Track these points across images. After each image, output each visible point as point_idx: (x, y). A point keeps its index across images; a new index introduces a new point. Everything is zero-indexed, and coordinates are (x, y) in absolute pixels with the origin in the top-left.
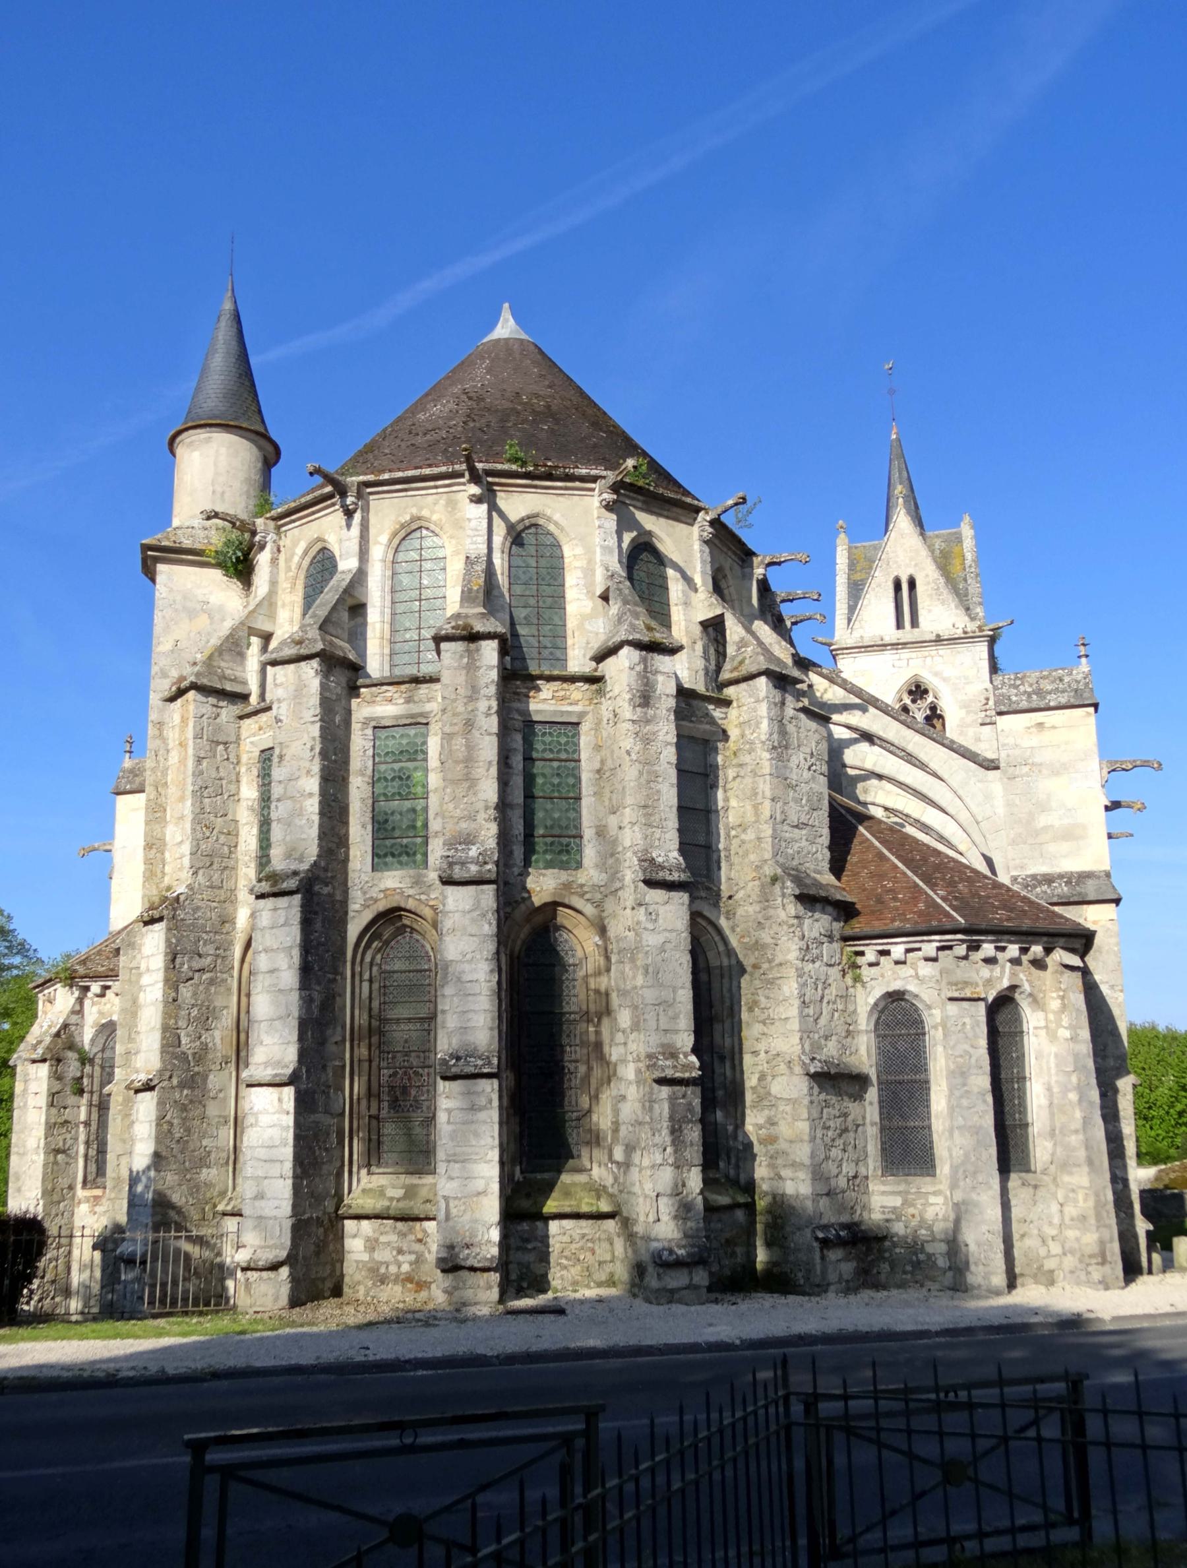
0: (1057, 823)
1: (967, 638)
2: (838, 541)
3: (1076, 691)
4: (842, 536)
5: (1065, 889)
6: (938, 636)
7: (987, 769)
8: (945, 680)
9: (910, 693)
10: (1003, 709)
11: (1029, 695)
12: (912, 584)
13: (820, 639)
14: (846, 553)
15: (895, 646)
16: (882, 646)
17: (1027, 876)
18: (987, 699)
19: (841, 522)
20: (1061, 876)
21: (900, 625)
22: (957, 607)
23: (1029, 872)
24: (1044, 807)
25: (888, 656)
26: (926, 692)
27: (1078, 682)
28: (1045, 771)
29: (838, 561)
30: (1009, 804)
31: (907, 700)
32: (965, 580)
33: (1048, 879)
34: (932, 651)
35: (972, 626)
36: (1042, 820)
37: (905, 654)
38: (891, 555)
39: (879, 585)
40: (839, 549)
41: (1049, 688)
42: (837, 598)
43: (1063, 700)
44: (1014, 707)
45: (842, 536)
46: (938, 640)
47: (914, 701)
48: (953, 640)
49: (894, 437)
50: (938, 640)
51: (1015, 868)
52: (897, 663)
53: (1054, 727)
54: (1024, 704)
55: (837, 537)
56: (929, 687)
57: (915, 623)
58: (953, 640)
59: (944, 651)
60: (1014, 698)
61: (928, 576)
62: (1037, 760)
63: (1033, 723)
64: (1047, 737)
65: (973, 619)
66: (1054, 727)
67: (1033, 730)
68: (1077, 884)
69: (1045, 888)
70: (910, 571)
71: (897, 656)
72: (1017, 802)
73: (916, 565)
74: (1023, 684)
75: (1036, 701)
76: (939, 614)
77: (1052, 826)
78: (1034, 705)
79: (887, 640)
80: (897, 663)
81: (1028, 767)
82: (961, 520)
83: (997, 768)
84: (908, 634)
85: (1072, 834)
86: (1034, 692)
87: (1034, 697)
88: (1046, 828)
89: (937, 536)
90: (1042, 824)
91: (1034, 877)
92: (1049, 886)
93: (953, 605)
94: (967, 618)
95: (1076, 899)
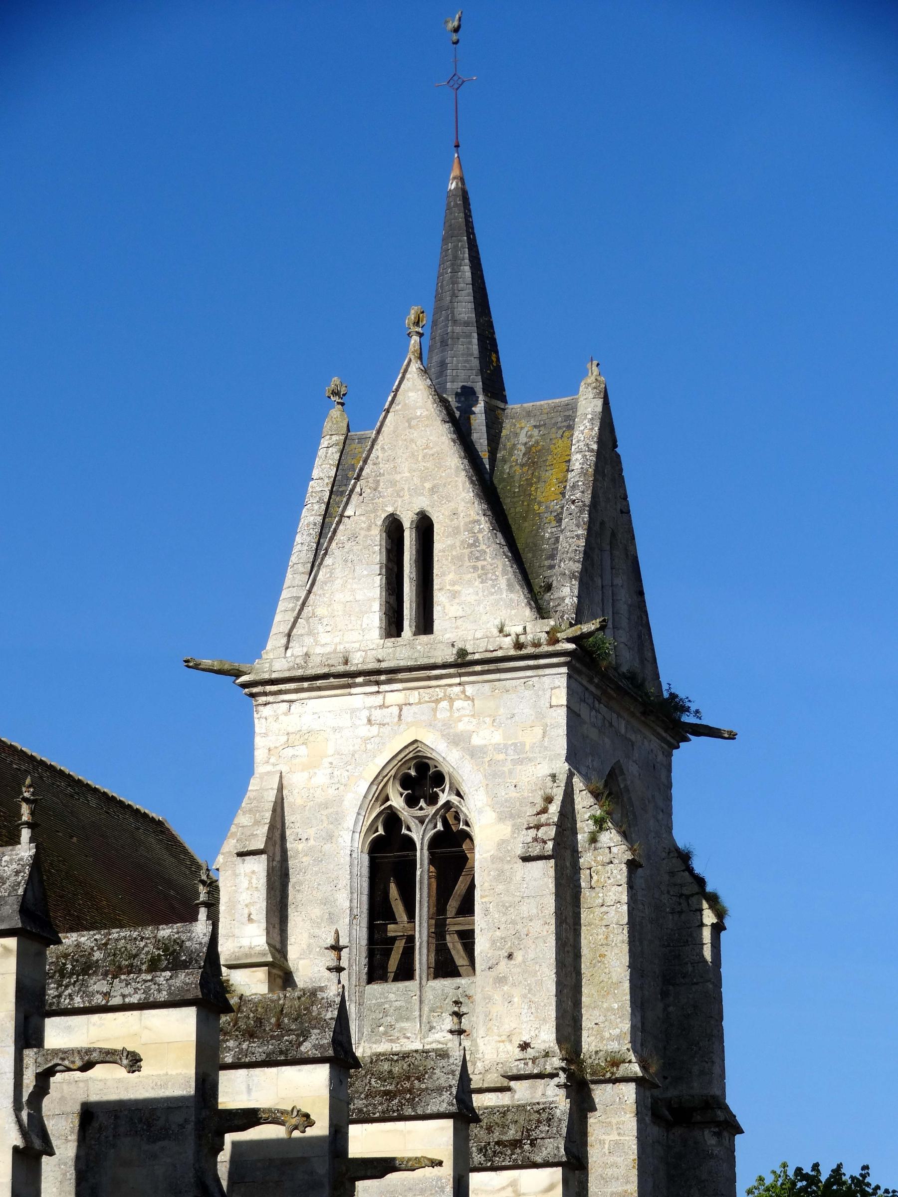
1: (522, 657)
2: (327, 425)
4: (335, 412)
6: (462, 653)
8: (474, 753)
9: (406, 782)
12: (425, 527)
13: (207, 662)
14: (334, 454)
15: (378, 675)
16: (343, 678)
18: (549, 800)
19: (336, 380)
21: (393, 625)
22: (510, 586)
25: (360, 699)
26: (439, 779)
29: (315, 473)
31: (397, 802)
32: (559, 520)
34: (451, 686)
35: (537, 630)
37: (395, 694)
38: (384, 467)
39: (354, 537)
40: (325, 442)
42: (294, 559)
46: (463, 663)
47: (411, 802)
48: (493, 664)
49: (452, 186)
50: (463, 663)
52: (377, 714)
55: (325, 415)
56: (445, 769)
57: (425, 625)
58: (493, 664)
59: (476, 688)
61: (458, 512)
65: (542, 612)
70: (422, 503)
71: (378, 700)
73: (433, 490)
76: (478, 602)
79: (358, 662)
80: (377, 714)
82: (584, 374)
84: (410, 648)
89: (529, 414)
93: (503, 582)
94: (528, 613)
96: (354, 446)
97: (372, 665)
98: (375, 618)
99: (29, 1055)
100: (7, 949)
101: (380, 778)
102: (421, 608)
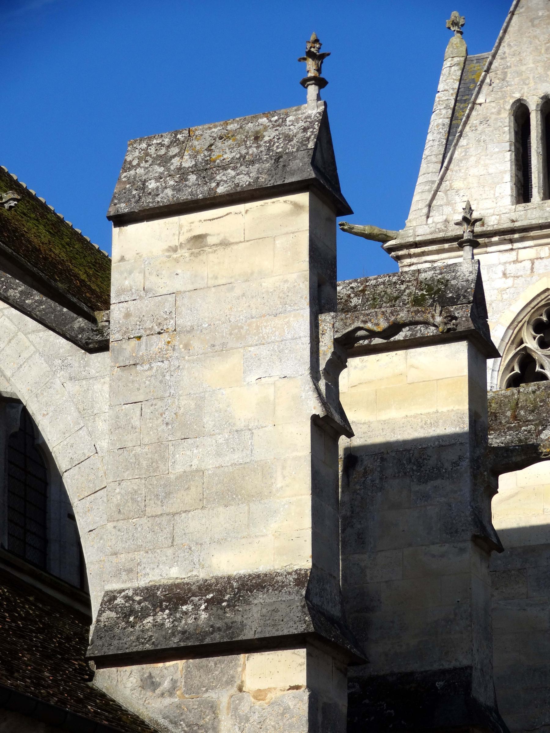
0: (210, 464)
2: (449, 50)
3: (279, 157)
4: (456, 39)
5: (204, 616)
7: (91, 351)
9: (538, 327)
10: (123, 208)
11: (183, 173)
14: (456, 72)
17: (136, 591)
19: (455, 14)
20: (205, 587)
21: (523, 194)
23: (143, 583)
24: (187, 431)
27: (288, 138)
28: (196, 344)
29: (441, 87)
30: (118, 427)
33: (175, 597)
36: (185, 458)
38: (511, 61)
39: (485, 120)
40: (447, 64)
41: (228, 156)
42: (426, 152)
43: (244, 180)
44: (148, 202)
45: (456, 39)
51: (117, 574)
52: (512, 269)
53: (225, 244)
54: (167, 196)
55: (446, 42)
60: (152, 185)
62: (185, 320)
63: (183, 238)
64: (213, 265)
66: (225, 244)
67: (184, 252)
68: (231, 605)
69: (163, 616)
71: (512, 256)
72: (136, 421)
74: (180, 154)
75: (194, 187)
77: (201, 472)
78: (185, 196)
80: (512, 269)
81: (165, 337)
83: (103, 346)
85: (236, 489)
86: (195, 169)
87: (193, 178)
88: (187, 477)
90: (179, 469)
91: (149, 593)
92: (174, 609)
95: (217, 638)
96: (473, 66)
97: (507, 225)
98: (506, 187)
99: (326, 320)
100: (297, 206)
101: (516, 323)
102: (547, 180)
